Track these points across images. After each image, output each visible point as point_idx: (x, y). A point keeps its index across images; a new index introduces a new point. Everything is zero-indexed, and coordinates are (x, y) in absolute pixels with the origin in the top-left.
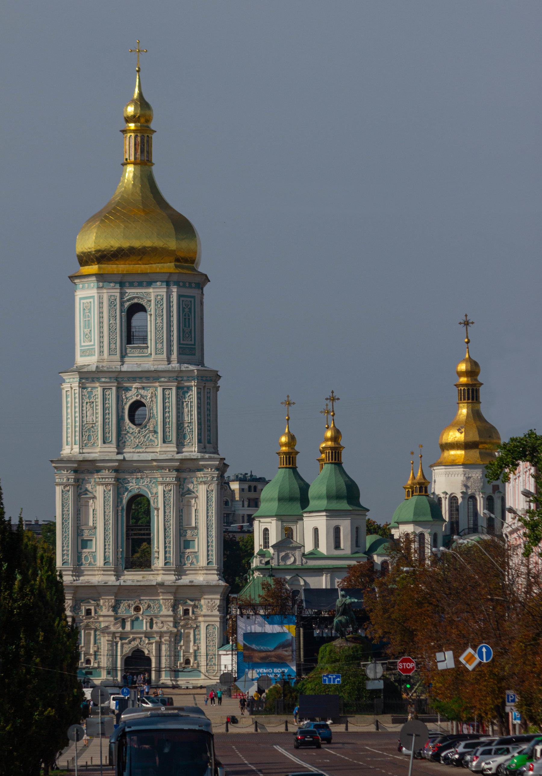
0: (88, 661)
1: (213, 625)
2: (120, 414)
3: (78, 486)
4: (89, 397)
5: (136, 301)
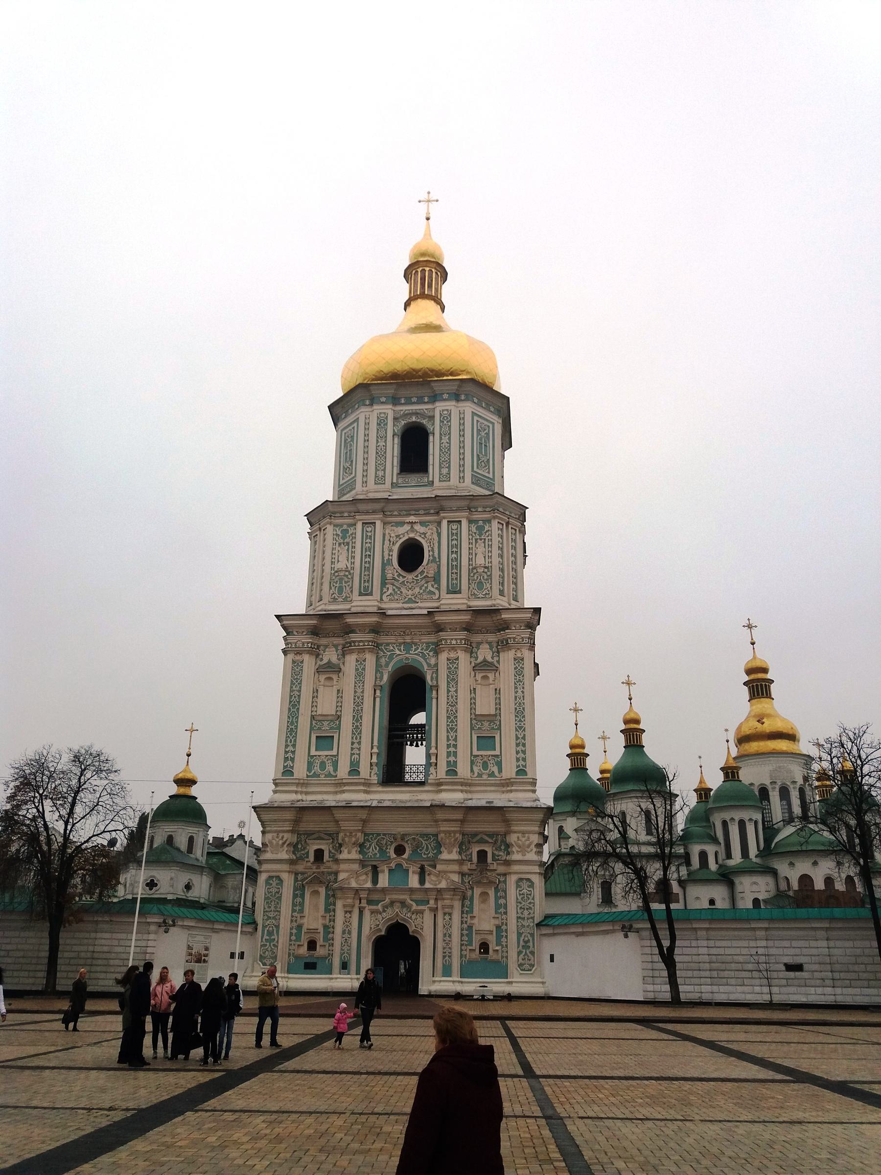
0: (312, 945)
1: (528, 880)
2: (386, 558)
3: (317, 655)
4: (344, 538)
5: (414, 419)
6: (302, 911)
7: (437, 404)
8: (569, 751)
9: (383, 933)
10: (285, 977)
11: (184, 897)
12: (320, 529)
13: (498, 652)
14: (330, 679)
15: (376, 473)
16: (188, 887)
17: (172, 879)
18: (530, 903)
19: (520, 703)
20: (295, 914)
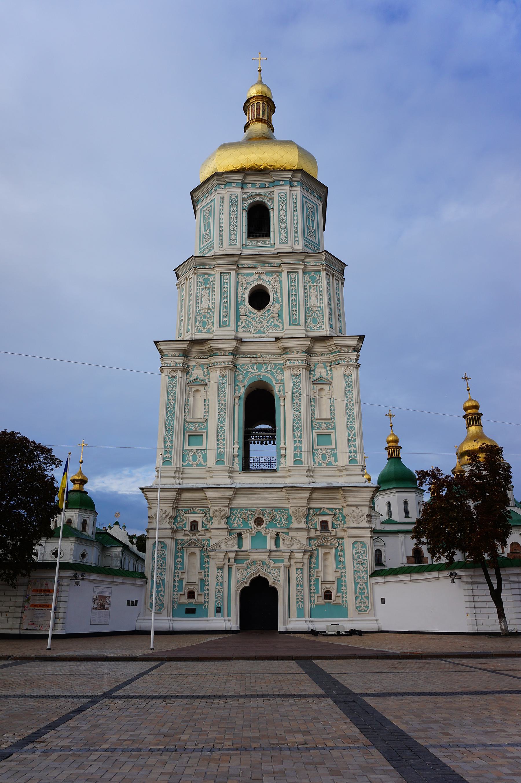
0: (191, 595)
2: (240, 299)
3: (188, 373)
4: (205, 284)
5: (258, 199)
6: (182, 568)
7: (276, 188)
8: (464, 413)
9: (248, 585)
10: (171, 620)
11: (81, 563)
12: (186, 279)
13: (331, 370)
14: (197, 391)
15: (230, 237)
16: (83, 555)
17: (71, 549)
18: (364, 560)
19: (350, 409)
20: (177, 571)
